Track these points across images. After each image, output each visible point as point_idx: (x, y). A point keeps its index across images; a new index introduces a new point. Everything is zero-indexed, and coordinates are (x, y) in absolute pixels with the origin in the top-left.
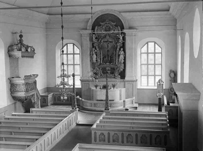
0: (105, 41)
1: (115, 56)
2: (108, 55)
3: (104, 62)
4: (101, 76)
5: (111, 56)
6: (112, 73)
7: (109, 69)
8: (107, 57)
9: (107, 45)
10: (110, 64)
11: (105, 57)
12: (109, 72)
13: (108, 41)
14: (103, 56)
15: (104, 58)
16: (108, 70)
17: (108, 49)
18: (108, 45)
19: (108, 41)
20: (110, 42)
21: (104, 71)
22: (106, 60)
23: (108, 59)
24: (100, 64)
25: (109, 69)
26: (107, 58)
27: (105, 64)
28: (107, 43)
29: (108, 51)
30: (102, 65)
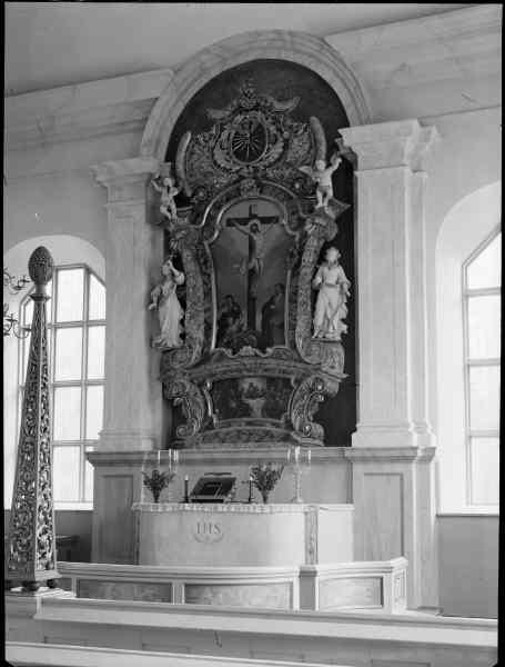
0: (237, 220)
1: (290, 301)
2: (252, 300)
3: (228, 345)
4: (208, 432)
5: (272, 301)
6: (273, 411)
7: (259, 384)
8: (244, 312)
9: (246, 237)
10: (264, 352)
11: (236, 315)
12: (256, 404)
13: (253, 216)
14: (225, 310)
15: (231, 320)
16: (253, 394)
17: (251, 266)
18: (251, 239)
19: (253, 216)
20: (265, 220)
21: (229, 400)
22: (240, 329)
23: (251, 322)
24: (206, 357)
25: (256, 389)
26: (244, 320)
27: (234, 353)
28: (247, 229)
29: (252, 272)
30: (218, 360)
